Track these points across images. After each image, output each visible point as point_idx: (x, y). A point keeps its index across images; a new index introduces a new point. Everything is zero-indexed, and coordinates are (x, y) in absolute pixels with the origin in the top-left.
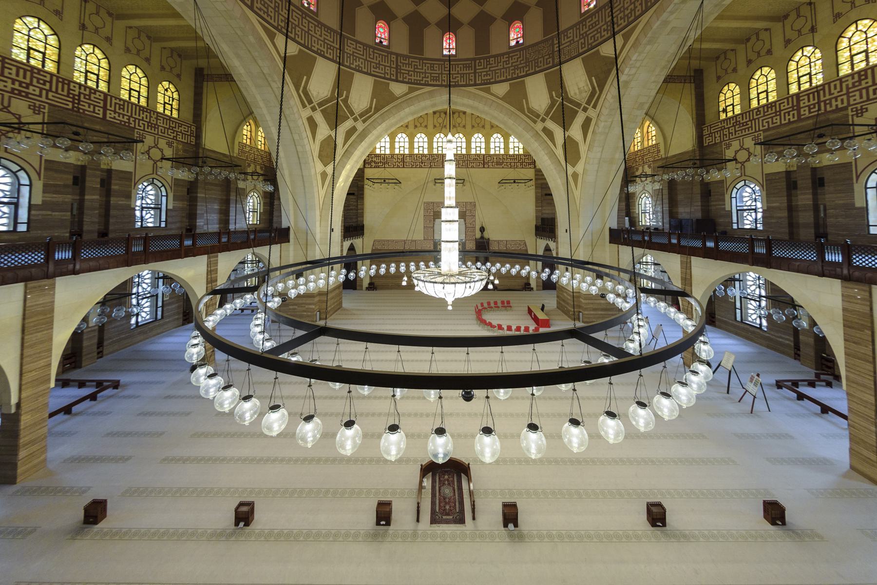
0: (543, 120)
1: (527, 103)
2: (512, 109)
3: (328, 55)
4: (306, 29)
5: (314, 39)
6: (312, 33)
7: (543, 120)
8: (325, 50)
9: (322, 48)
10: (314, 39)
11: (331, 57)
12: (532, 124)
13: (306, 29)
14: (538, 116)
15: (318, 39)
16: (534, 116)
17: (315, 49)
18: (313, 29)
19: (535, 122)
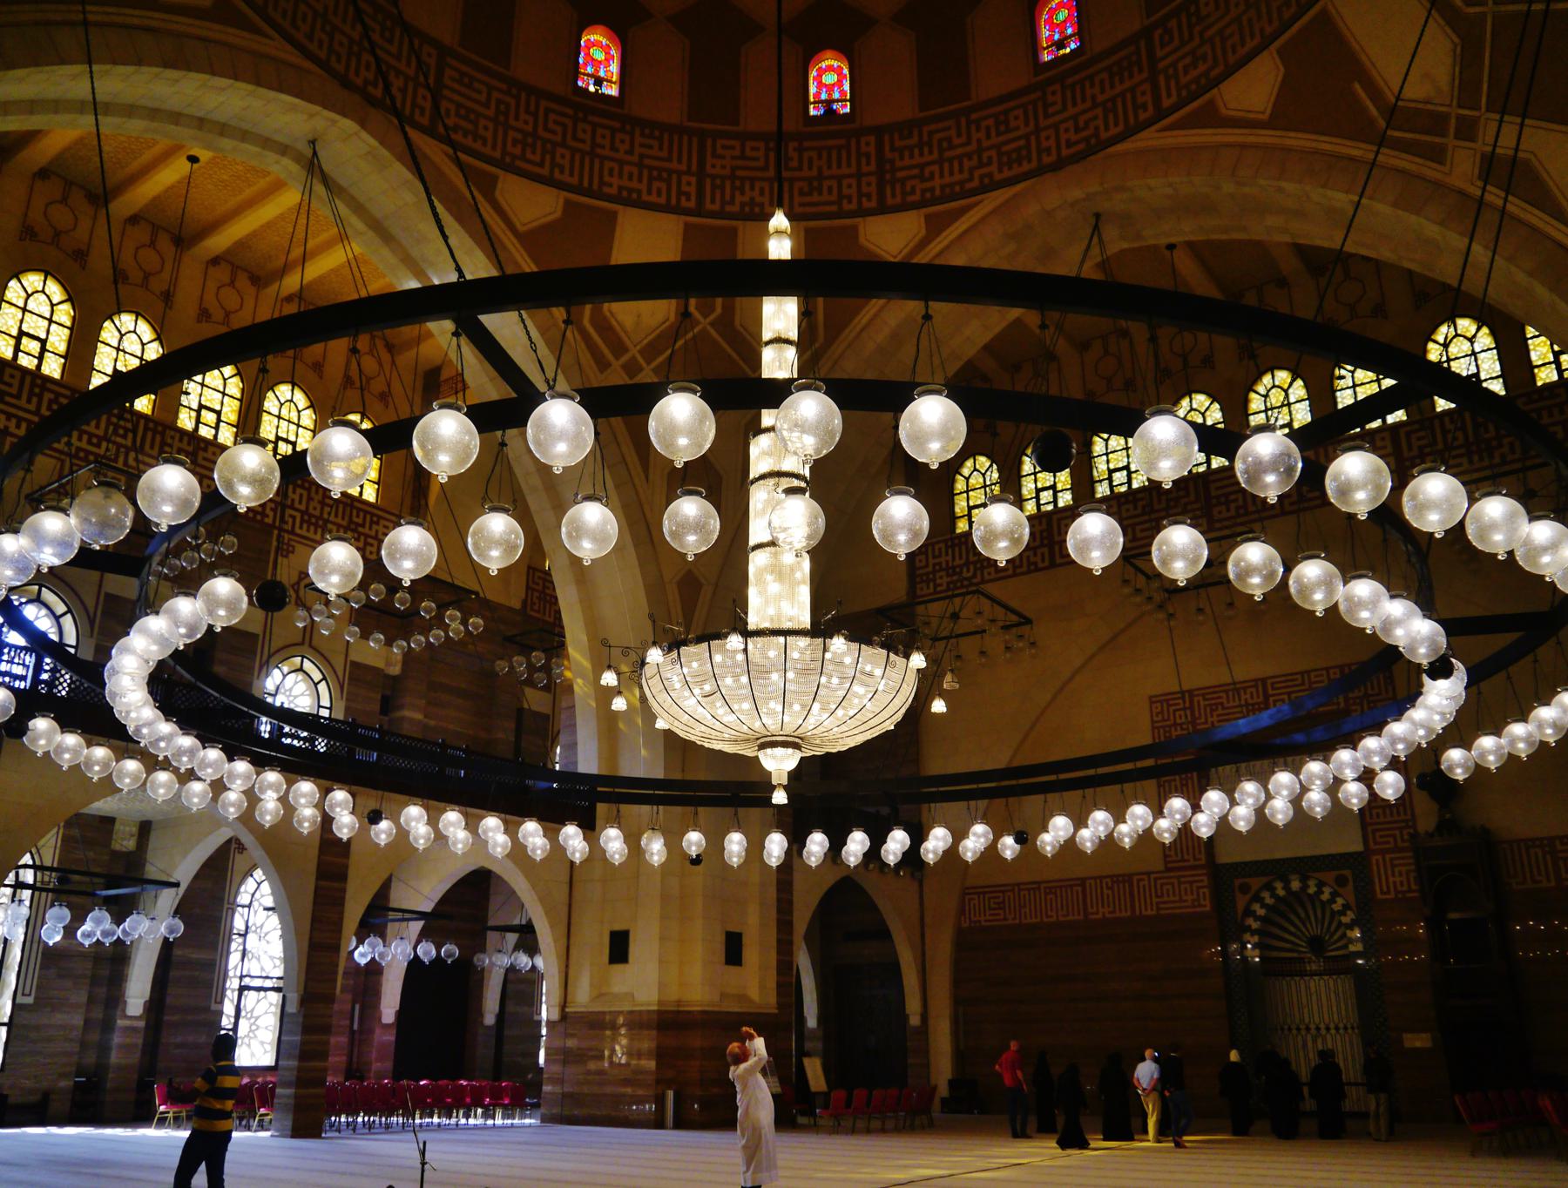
0: (1467, 131)
1: (1375, 93)
2: (1327, 144)
3: (653, 198)
4: (587, 148)
5: (608, 164)
6: (607, 152)
7: (1467, 131)
8: (643, 187)
9: (634, 184)
10: (608, 164)
11: (662, 200)
12: (1431, 171)
13: (587, 148)
14: (1436, 123)
15: (621, 163)
16: (1418, 129)
17: (613, 191)
18: (607, 143)
19: (1436, 155)
